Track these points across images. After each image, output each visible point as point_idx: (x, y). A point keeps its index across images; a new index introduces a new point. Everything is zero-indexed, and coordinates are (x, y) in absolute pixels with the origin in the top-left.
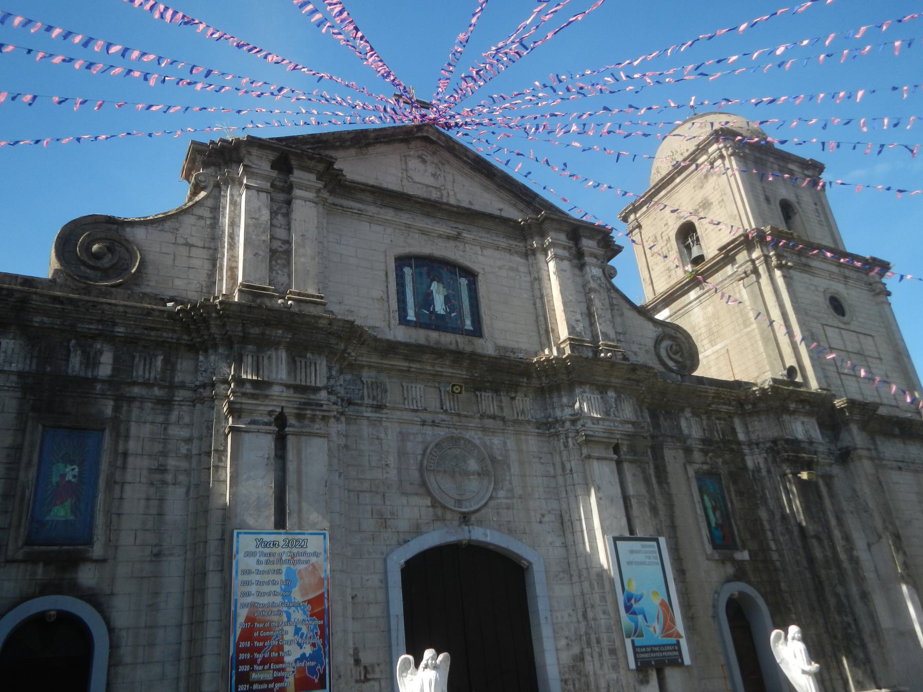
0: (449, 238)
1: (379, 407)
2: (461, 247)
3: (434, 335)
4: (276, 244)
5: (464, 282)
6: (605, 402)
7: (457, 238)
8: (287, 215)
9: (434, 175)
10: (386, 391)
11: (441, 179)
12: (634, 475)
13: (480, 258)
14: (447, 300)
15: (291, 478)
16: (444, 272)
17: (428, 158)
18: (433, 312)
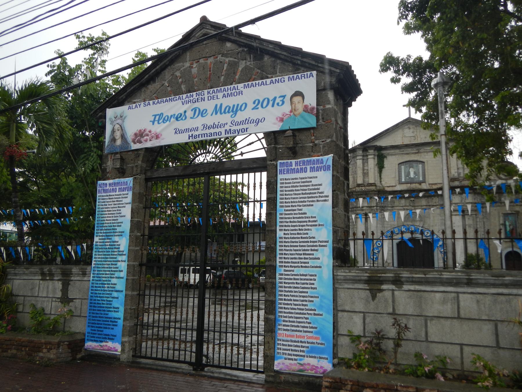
0: (416, 153)
1: (393, 207)
2: (420, 154)
3: (409, 185)
4: (365, 171)
5: (420, 166)
6: (462, 197)
7: (418, 153)
8: (367, 163)
9: (413, 132)
10: (394, 202)
11: (415, 133)
12: (469, 219)
13: (426, 157)
14: (415, 173)
15: (369, 227)
16: (414, 164)
17: (411, 127)
18: (410, 178)
